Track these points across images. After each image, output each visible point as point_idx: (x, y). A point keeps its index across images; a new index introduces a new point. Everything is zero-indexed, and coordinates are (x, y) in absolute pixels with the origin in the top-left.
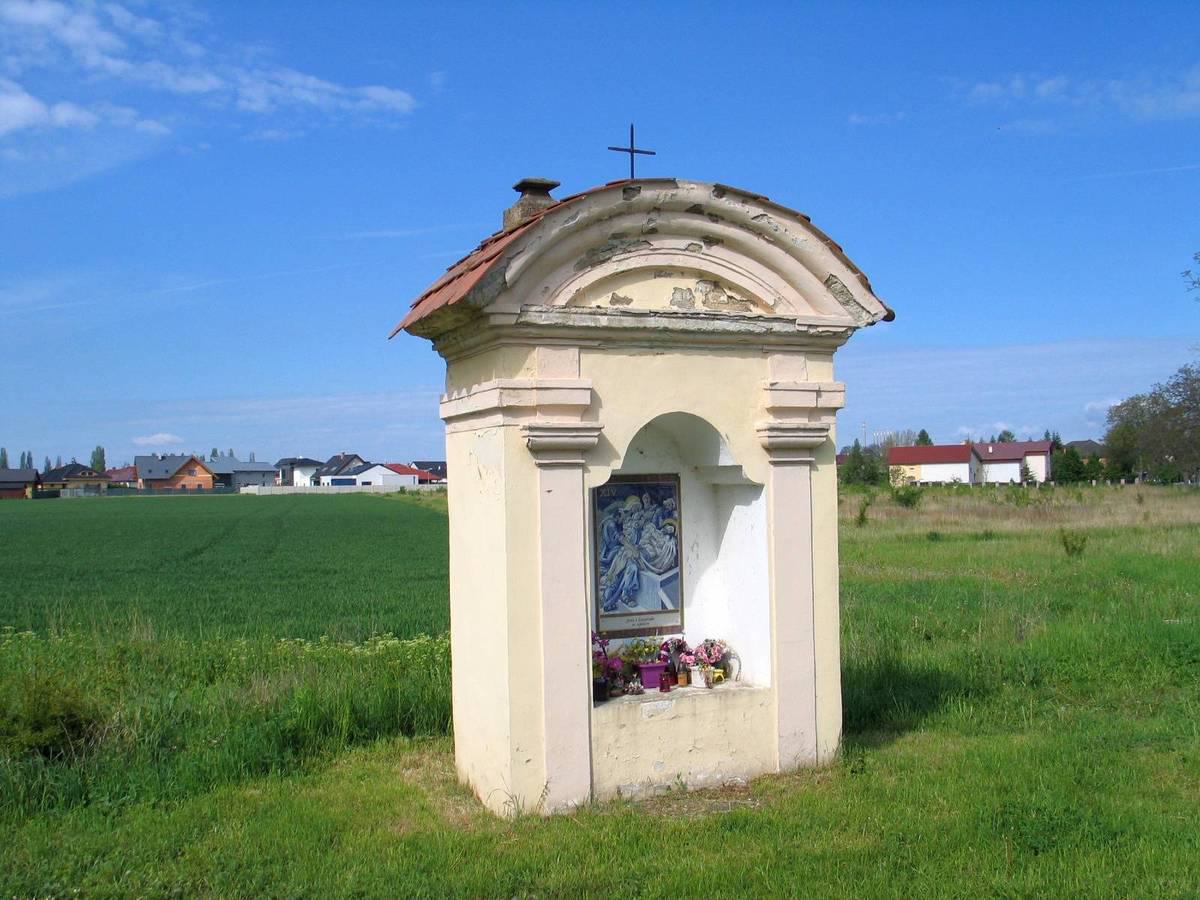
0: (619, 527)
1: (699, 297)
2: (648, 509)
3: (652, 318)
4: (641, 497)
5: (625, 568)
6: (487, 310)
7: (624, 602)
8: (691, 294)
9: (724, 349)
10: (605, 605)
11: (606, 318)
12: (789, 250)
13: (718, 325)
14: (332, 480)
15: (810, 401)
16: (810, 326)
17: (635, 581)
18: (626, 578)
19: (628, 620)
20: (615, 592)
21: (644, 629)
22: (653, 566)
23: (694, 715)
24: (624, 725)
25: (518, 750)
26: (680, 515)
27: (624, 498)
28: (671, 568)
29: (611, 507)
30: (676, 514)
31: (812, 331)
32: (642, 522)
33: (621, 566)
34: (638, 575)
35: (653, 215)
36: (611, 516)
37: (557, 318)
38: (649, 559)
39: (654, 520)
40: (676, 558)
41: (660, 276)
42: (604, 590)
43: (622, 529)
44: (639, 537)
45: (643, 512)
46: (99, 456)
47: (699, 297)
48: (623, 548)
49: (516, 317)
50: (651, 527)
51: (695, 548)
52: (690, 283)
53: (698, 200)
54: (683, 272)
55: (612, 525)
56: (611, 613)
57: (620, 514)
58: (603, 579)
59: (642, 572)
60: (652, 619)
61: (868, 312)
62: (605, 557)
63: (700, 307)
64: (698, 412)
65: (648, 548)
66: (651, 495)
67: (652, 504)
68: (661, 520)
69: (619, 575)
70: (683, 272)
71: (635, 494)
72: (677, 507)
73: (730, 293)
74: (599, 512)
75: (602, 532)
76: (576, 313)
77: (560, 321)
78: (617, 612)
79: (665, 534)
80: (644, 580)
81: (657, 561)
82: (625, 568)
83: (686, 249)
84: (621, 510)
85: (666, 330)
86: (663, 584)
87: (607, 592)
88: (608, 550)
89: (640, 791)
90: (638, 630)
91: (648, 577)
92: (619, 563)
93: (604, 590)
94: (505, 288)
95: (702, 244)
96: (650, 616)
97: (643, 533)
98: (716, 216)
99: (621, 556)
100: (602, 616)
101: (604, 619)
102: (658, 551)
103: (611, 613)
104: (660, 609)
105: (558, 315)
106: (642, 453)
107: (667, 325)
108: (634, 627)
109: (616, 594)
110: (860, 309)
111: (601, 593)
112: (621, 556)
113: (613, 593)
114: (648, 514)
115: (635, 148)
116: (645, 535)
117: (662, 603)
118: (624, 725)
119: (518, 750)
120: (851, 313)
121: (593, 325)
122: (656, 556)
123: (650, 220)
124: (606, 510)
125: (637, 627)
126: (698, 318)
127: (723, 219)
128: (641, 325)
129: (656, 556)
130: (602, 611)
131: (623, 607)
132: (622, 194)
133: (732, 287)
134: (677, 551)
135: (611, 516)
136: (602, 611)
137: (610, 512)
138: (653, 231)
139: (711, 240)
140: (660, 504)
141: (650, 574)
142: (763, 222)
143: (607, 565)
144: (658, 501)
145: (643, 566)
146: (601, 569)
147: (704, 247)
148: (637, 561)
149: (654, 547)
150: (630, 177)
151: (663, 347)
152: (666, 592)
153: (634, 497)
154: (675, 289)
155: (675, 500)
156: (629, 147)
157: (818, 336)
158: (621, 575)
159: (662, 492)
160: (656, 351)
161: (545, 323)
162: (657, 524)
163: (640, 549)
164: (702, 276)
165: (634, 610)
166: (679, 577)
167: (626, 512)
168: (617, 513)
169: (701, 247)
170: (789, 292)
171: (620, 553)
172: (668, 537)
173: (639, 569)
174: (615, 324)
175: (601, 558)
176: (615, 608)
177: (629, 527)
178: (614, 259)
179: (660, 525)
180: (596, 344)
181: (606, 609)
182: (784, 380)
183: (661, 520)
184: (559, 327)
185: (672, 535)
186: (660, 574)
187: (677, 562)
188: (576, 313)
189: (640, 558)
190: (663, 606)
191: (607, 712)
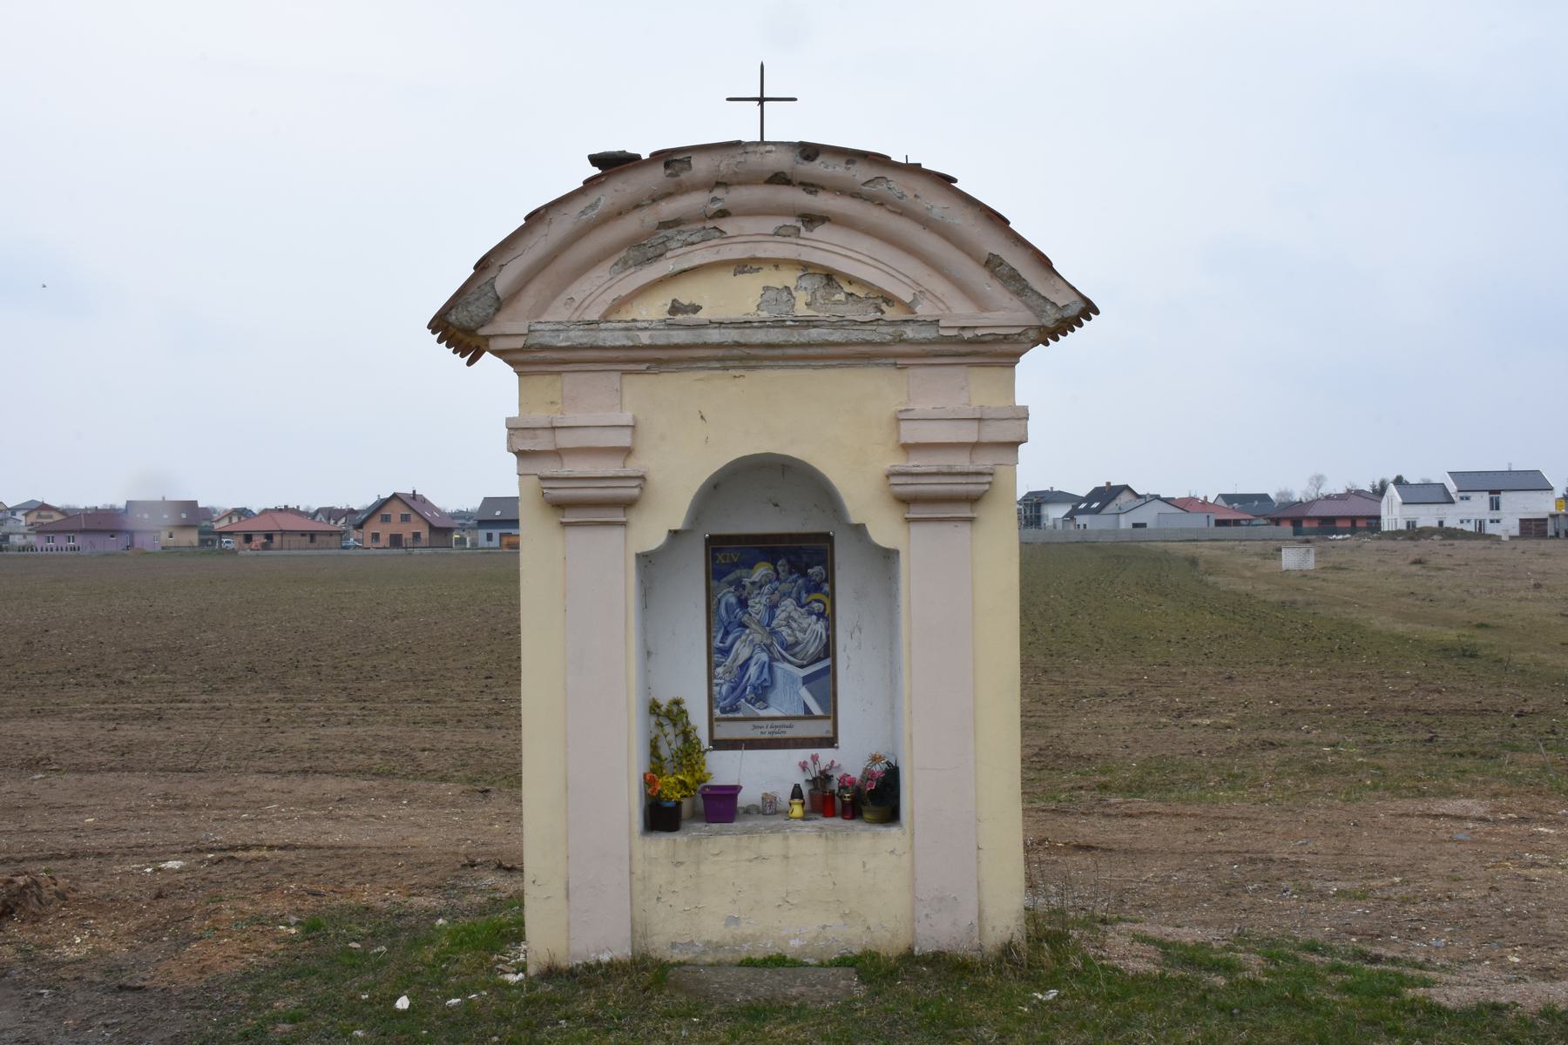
0: (743, 603)
1: (801, 298)
2: (785, 581)
3: (717, 331)
4: (774, 563)
5: (750, 658)
6: (483, 332)
7: (749, 702)
8: (790, 294)
9: (833, 366)
10: (721, 704)
11: (648, 333)
12: (927, 223)
13: (814, 334)
14: (501, 534)
15: (968, 434)
16: (963, 328)
17: (766, 675)
18: (753, 670)
19: (755, 727)
20: (737, 688)
21: (777, 740)
22: (793, 655)
23: (786, 857)
24: (681, 863)
25: (534, 882)
26: (833, 587)
27: (751, 566)
28: (818, 660)
29: (731, 577)
30: (826, 588)
31: (967, 335)
32: (776, 597)
33: (744, 653)
34: (771, 668)
35: (718, 193)
36: (732, 589)
37: (581, 337)
38: (788, 647)
39: (794, 595)
40: (827, 646)
41: (743, 272)
42: (721, 685)
43: (747, 606)
44: (772, 617)
45: (777, 583)
46: (298, 507)
47: (801, 298)
48: (747, 631)
49: (524, 338)
50: (788, 604)
51: (857, 634)
52: (788, 278)
53: (778, 168)
54: (777, 264)
55: (733, 600)
56: (730, 715)
57: (744, 587)
58: (720, 670)
59: (775, 664)
60: (790, 727)
61: (1054, 304)
62: (722, 641)
63: (801, 310)
64: (795, 452)
65: (785, 631)
66: (789, 562)
67: (791, 573)
68: (804, 595)
69: (741, 666)
70: (777, 264)
71: (767, 560)
72: (830, 578)
73: (848, 289)
74: (714, 583)
75: (718, 608)
76: (606, 330)
77: (585, 340)
78: (740, 715)
79: (810, 613)
80: (779, 674)
81: (797, 649)
82: (750, 658)
83: (776, 234)
84: (746, 581)
85: (738, 345)
86: (807, 680)
87: (725, 688)
88: (727, 633)
89: (704, 952)
90: (770, 740)
91: (785, 671)
92: (742, 651)
93: (721, 685)
94: (499, 304)
95: (799, 224)
96: (787, 723)
97: (778, 612)
98: (812, 185)
99: (745, 641)
100: (718, 720)
101: (724, 724)
102: (800, 635)
103: (730, 715)
104: (802, 713)
105: (581, 333)
106: (776, 505)
107: (737, 338)
108: (764, 736)
109: (739, 691)
110: (1042, 301)
111: (716, 689)
112: (745, 641)
113: (734, 689)
114: (785, 587)
115: (759, 96)
116: (781, 615)
117: (805, 705)
118: (681, 863)
119: (534, 882)
120: (1030, 307)
121: (631, 344)
122: (797, 643)
123: (714, 200)
124: (722, 581)
125: (767, 736)
126: (783, 327)
127: (823, 188)
128: (700, 341)
129: (797, 643)
130: (717, 712)
131: (747, 709)
132: (662, 168)
133: (851, 280)
134: (828, 636)
135: (732, 589)
136: (717, 712)
137: (730, 584)
138: (723, 214)
139: (811, 219)
140: (804, 574)
141: (786, 666)
142: (881, 188)
143: (725, 652)
144: (798, 567)
145: (777, 655)
146: (716, 657)
147: (803, 229)
148: (768, 648)
149: (793, 630)
150: (759, 140)
151: (744, 368)
152: (810, 691)
153: (763, 563)
154: (766, 289)
155: (826, 569)
156: (759, 96)
157: (977, 341)
158: (745, 666)
159: (805, 559)
160: (732, 372)
161: (563, 344)
162: (798, 600)
163: (773, 633)
164: (806, 267)
165: (763, 713)
166: (831, 672)
167: (753, 583)
168: (739, 585)
169: (799, 230)
170: (938, 285)
171: (743, 637)
172: (814, 617)
173: (772, 659)
174: (662, 341)
175: (717, 643)
176: (737, 710)
177: (758, 604)
178: (669, 254)
179: (804, 601)
180: (643, 367)
181: (723, 711)
182: (922, 407)
183: (804, 595)
184: (587, 348)
185: (820, 615)
186: (802, 667)
187: (828, 650)
188: (606, 330)
189: (772, 644)
190: (807, 709)
191: (662, 843)
